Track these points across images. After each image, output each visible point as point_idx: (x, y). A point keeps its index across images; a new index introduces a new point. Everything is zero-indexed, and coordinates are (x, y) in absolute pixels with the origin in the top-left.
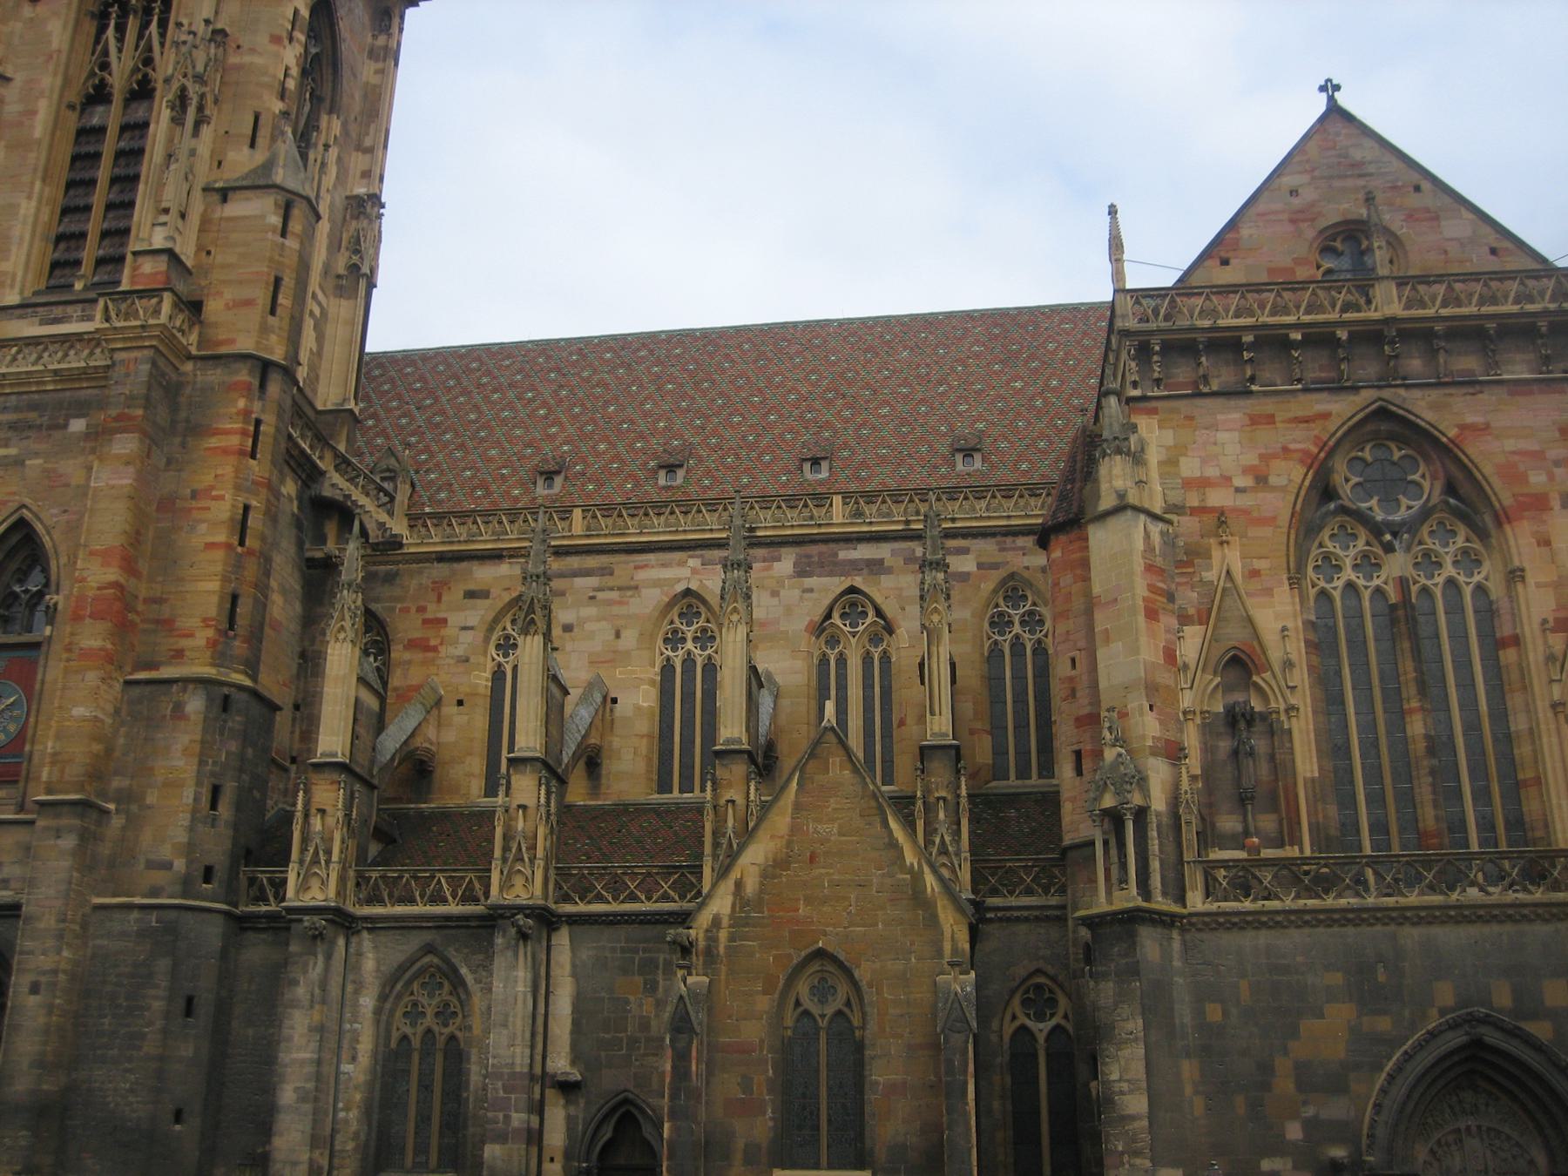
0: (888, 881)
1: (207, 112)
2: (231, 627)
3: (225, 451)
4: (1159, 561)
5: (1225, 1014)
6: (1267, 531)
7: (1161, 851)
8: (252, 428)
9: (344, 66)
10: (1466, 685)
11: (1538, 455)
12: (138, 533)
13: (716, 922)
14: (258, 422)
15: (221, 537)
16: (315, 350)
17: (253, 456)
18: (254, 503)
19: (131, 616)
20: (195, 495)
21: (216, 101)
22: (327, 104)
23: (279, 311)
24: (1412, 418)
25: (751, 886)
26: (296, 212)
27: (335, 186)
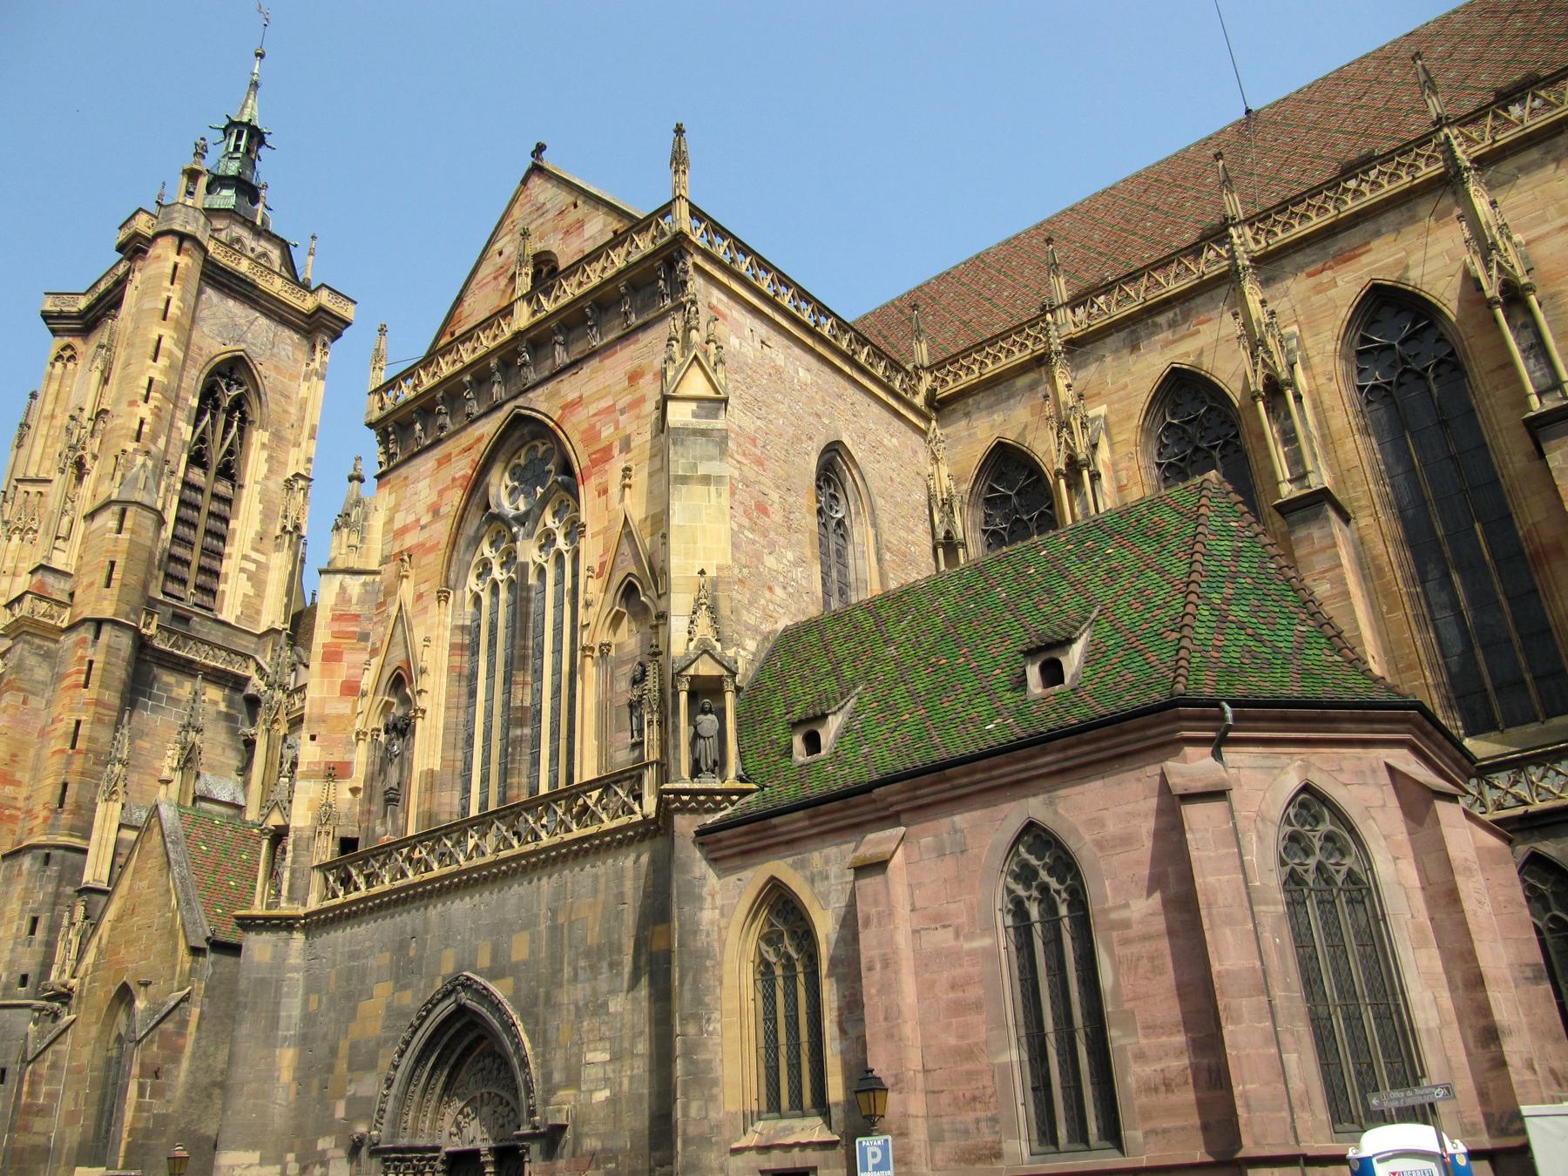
0: (162, 920)
1: (88, 466)
2: (61, 806)
3: (69, 688)
4: (355, 609)
5: (320, 1001)
6: (431, 557)
7: (294, 862)
8: (85, 668)
9: (270, 394)
10: (557, 651)
11: (610, 410)
12: (14, 755)
13: (87, 970)
14: (91, 663)
15: (59, 747)
16: (251, 592)
17: (86, 686)
18: (83, 718)
19: (7, 812)
20: (53, 723)
21: (95, 457)
22: (257, 424)
23: (113, 584)
24: (534, 414)
25: (104, 941)
26: (128, 514)
27: (267, 478)
